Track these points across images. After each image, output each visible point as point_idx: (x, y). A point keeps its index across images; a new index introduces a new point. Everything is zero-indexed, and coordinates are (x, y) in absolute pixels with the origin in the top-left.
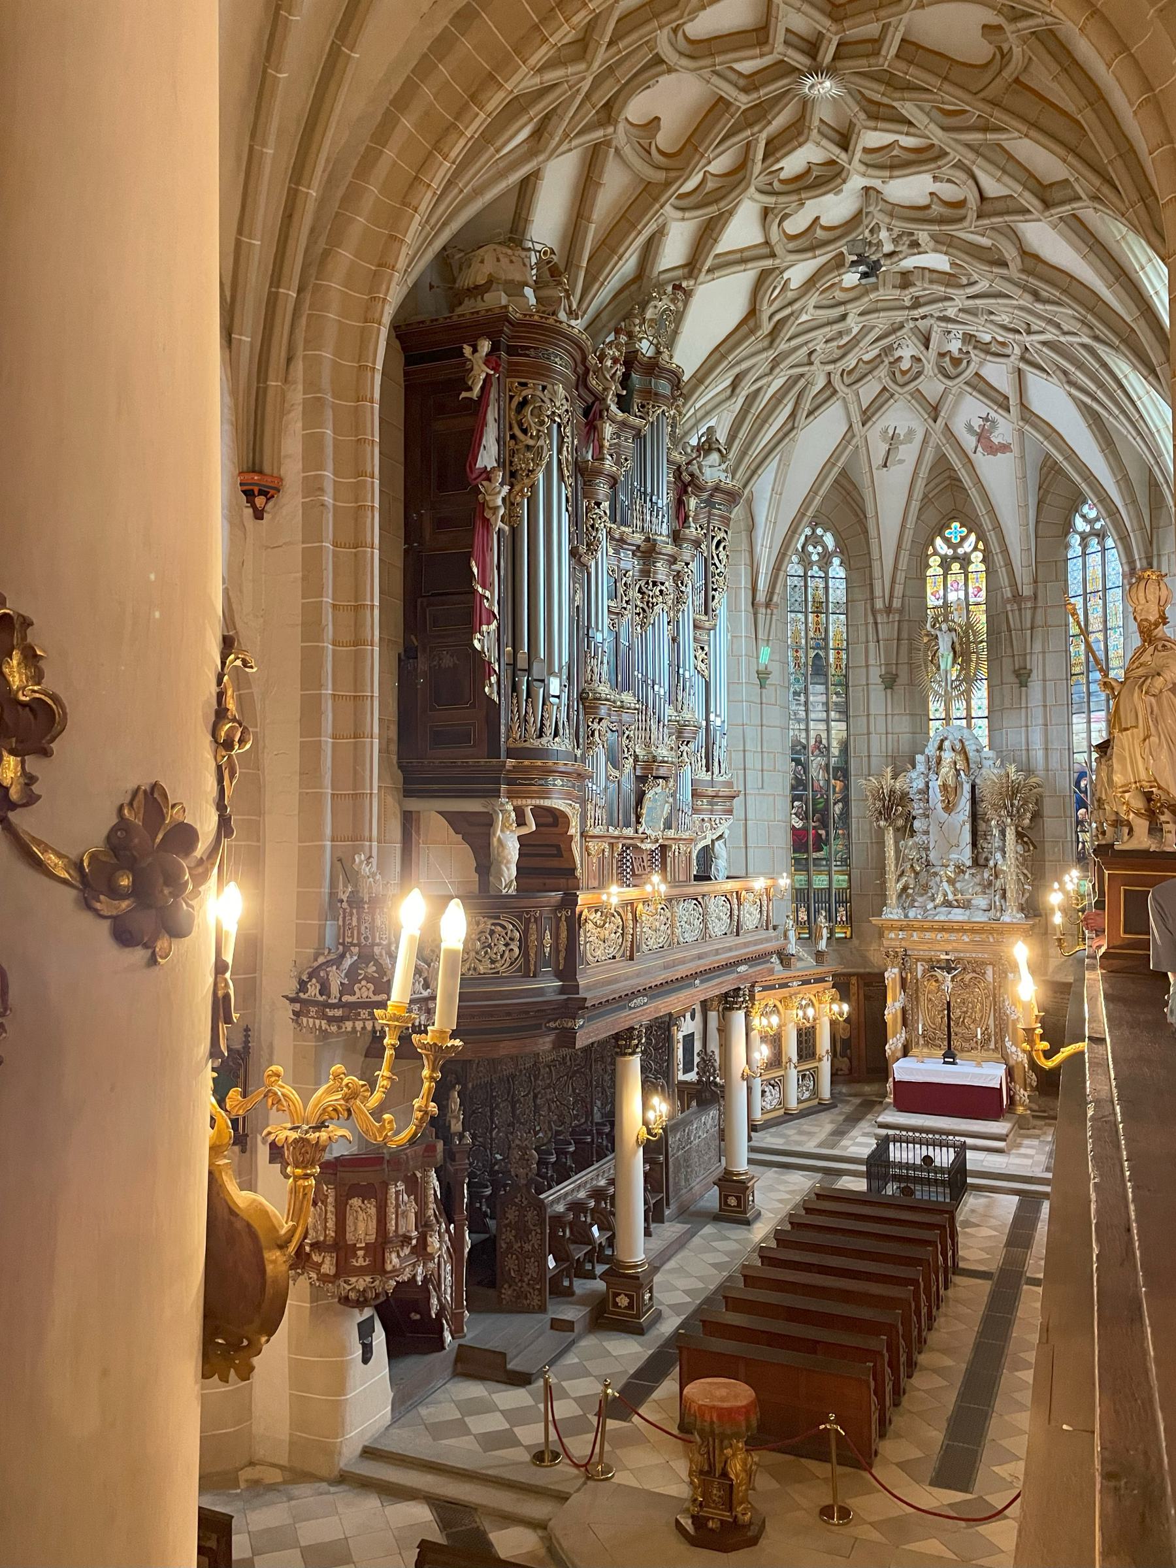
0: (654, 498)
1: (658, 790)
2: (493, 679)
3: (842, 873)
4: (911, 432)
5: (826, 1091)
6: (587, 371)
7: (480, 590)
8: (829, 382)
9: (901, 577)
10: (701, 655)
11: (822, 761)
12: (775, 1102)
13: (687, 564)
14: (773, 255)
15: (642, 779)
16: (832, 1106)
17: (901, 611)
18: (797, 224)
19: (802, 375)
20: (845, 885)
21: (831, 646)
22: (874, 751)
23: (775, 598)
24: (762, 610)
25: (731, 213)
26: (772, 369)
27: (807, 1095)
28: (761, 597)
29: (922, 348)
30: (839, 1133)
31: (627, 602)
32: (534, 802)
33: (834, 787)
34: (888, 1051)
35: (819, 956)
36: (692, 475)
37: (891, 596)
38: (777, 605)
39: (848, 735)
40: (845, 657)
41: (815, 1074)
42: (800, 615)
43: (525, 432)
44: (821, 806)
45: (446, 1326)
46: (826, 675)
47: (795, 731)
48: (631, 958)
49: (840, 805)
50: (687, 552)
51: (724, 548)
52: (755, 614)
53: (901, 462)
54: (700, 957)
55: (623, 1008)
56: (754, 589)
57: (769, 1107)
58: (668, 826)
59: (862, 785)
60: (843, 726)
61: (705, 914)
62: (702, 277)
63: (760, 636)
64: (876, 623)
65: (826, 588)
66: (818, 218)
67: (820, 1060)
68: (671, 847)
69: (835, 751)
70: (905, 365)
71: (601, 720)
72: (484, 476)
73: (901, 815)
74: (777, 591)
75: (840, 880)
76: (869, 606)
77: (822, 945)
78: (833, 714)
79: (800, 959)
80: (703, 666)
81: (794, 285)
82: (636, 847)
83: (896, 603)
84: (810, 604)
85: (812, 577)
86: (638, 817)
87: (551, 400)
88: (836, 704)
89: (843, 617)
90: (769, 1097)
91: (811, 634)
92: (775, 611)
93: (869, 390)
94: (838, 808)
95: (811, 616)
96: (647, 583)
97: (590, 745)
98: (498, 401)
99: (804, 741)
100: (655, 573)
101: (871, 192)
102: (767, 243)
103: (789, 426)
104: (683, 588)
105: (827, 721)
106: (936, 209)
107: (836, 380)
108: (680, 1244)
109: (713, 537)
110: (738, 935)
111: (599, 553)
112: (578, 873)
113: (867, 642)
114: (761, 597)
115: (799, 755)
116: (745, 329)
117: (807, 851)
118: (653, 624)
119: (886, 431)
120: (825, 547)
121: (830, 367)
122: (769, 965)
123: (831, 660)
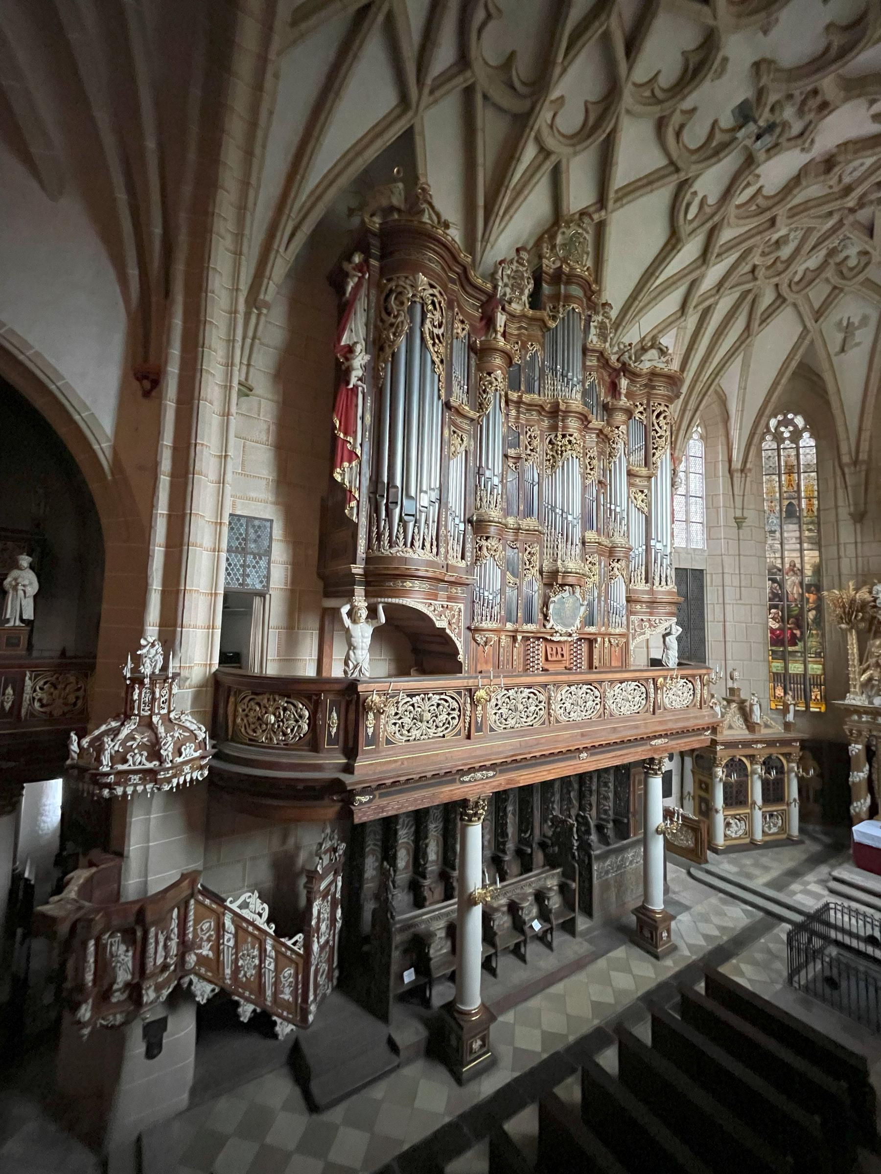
0: (565, 372)
1: (566, 595)
2: (353, 504)
3: (816, 663)
4: (865, 320)
5: (795, 831)
6: (465, 270)
7: (342, 436)
8: (779, 295)
9: (866, 435)
10: (641, 497)
11: (796, 579)
12: (741, 832)
13: (618, 428)
14: (677, 170)
15: (549, 585)
16: (800, 842)
17: (869, 462)
18: (695, 135)
19: (749, 291)
20: (819, 672)
21: (803, 494)
22: (845, 570)
23: (748, 465)
24: (737, 475)
25: (614, 131)
26: (718, 291)
27: (774, 830)
28: (737, 464)
29: (867, 239)
30: (794, 874)
31: (532, 450)
32: (383, 600)
33: (808, 599)
34: (852, 811)
35: (787, 726)
36: (624, 364)
37: (857, 452)
38: (750, 470)
39: (821, 560)
40: (816, 502)
41: (784, 815)
42: (774, 477)
43: (389, 314)
44: (796, 612)
45: (279, 1021)
46: (799, 518)
47: (772, 559)
48: (469, 737)
49: (814, 612)
50: (620, 417)
51: (665, 418)
52: (732, 478)
53: (858, 344)
54: (583, 735)
55: (453, 781)
56: (730, 461)
57: (733, 835)
58: (590, 620)
59: (831, 595)
60: (816, 553)
61: (603, 697)
62: (611, 205)
63: (736, 493)
64: (844, 474)
65: (798, 455)
66: (715, 123)
67: (788, 804)
68: (596, 640)
69: (808, 571)
70: (852, 263)
71: (487, 538)
72: (346, 349)
73: (863, 619)
74: (749, 460)
75: (815, 668)
76: (836, 464)
77: (790, 717)
78: (805, 545)
79: (767, 726)
80: (643, 505)
81: (711, 201)
82: (545, 639)
83: (863, 456)
84: (783, 468)
85: (784, 449)
86: (545, 616)
87: (412, 286)
88: (808, 537)
89: (814, 474)
90: (734, 828)
91: (785, 489)
92: (749, 474)
93: (818, 293)
94: (811, 615)
95: (783, 477)
96: (556, 436)
97: (477, 559)
98: (368, 296)
99: (780, 566)
100: (565, 428)
101: (763, 67)
102: (672, 163)
103: (746, 335)
104: (614, 446)
105: (801, 550)
106: (837, 41)
107: (784, 290)
108: (579, 965)
109: (653, 411)
110: (654, 713)
111: (491, 408)
112: (461, 657)
113: (836, 488)
114: (737, 464)
115: (775, 576)
116: (669, 247)
117: (783, 645)
118: (563, 466)
119: (841, 320)
120: (796, 426)
121: (776, 280)
122: (703, 737)
123: (803, 506)
